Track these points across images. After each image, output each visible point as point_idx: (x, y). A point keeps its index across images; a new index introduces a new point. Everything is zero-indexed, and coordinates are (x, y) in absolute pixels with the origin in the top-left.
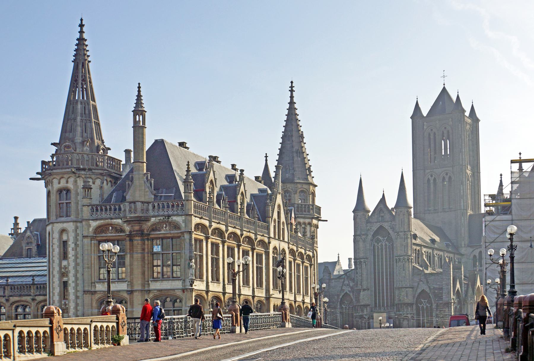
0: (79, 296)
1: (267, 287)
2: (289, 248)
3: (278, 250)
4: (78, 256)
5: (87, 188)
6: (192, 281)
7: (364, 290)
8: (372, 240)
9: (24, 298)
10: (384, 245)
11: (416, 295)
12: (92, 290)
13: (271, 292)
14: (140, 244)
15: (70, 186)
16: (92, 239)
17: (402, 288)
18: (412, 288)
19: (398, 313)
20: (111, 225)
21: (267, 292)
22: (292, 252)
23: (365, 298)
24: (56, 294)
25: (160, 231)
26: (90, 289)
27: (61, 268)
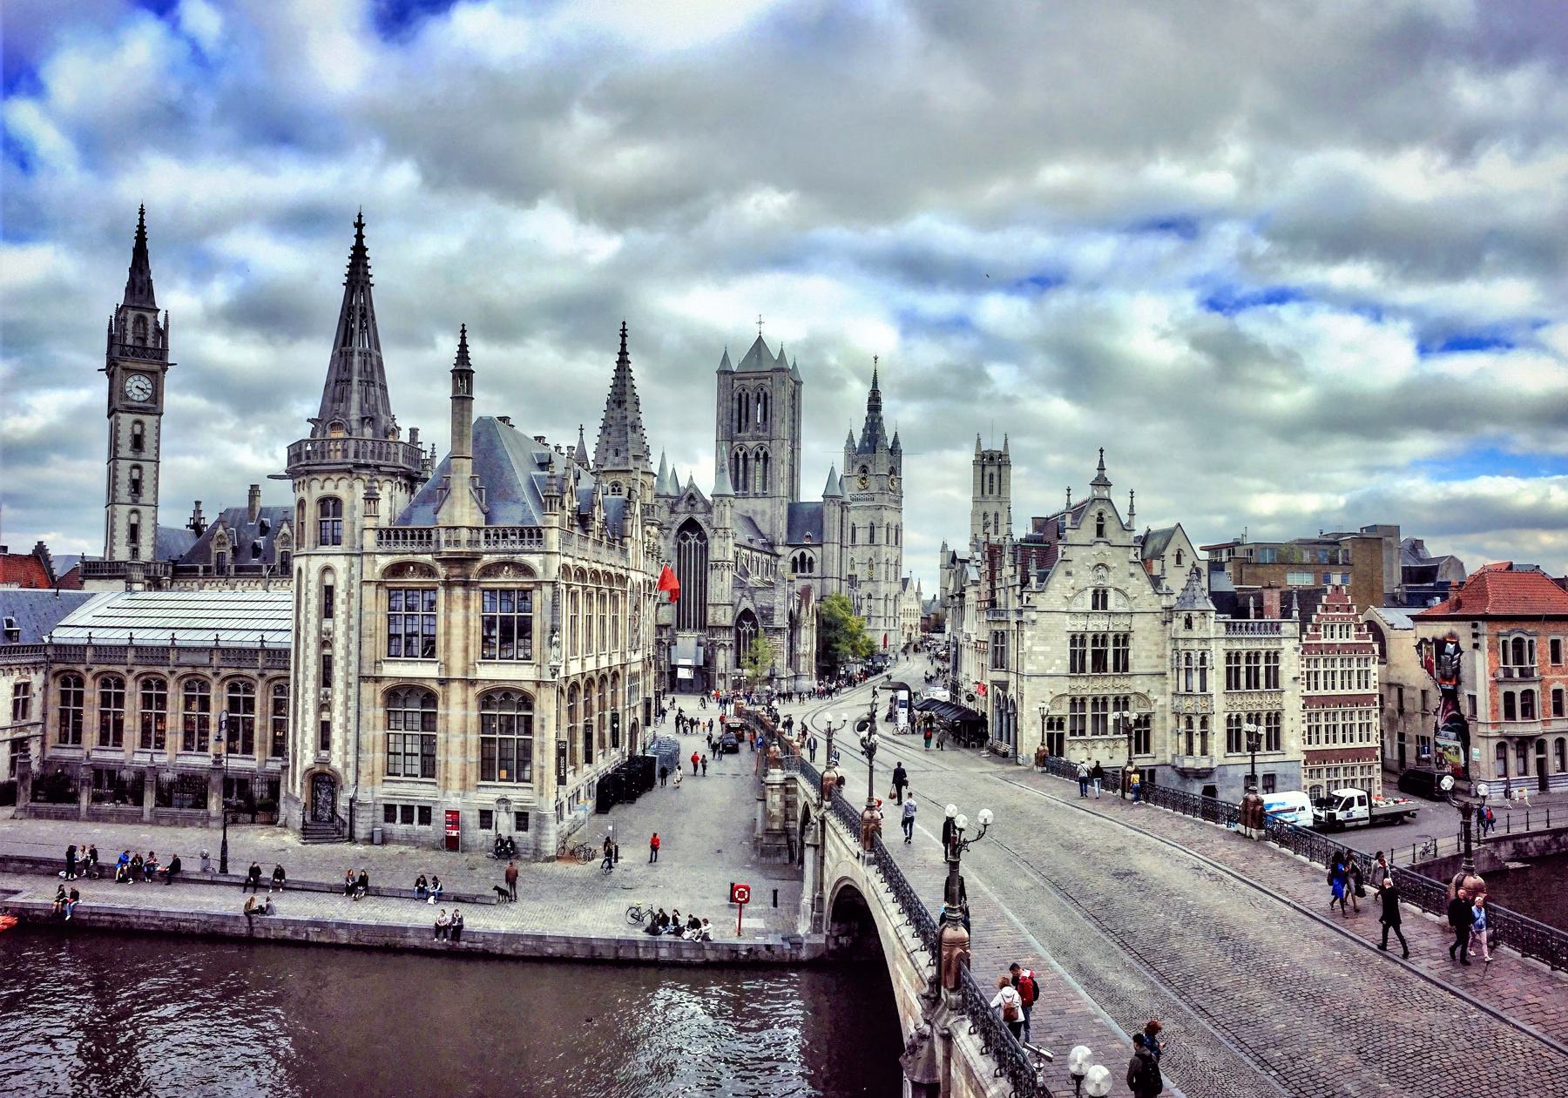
5: (371, 498)
15: (342, 492)
20: (412, 563)
24: (311, 677)
25: (496, 576)
27: (320, 632)
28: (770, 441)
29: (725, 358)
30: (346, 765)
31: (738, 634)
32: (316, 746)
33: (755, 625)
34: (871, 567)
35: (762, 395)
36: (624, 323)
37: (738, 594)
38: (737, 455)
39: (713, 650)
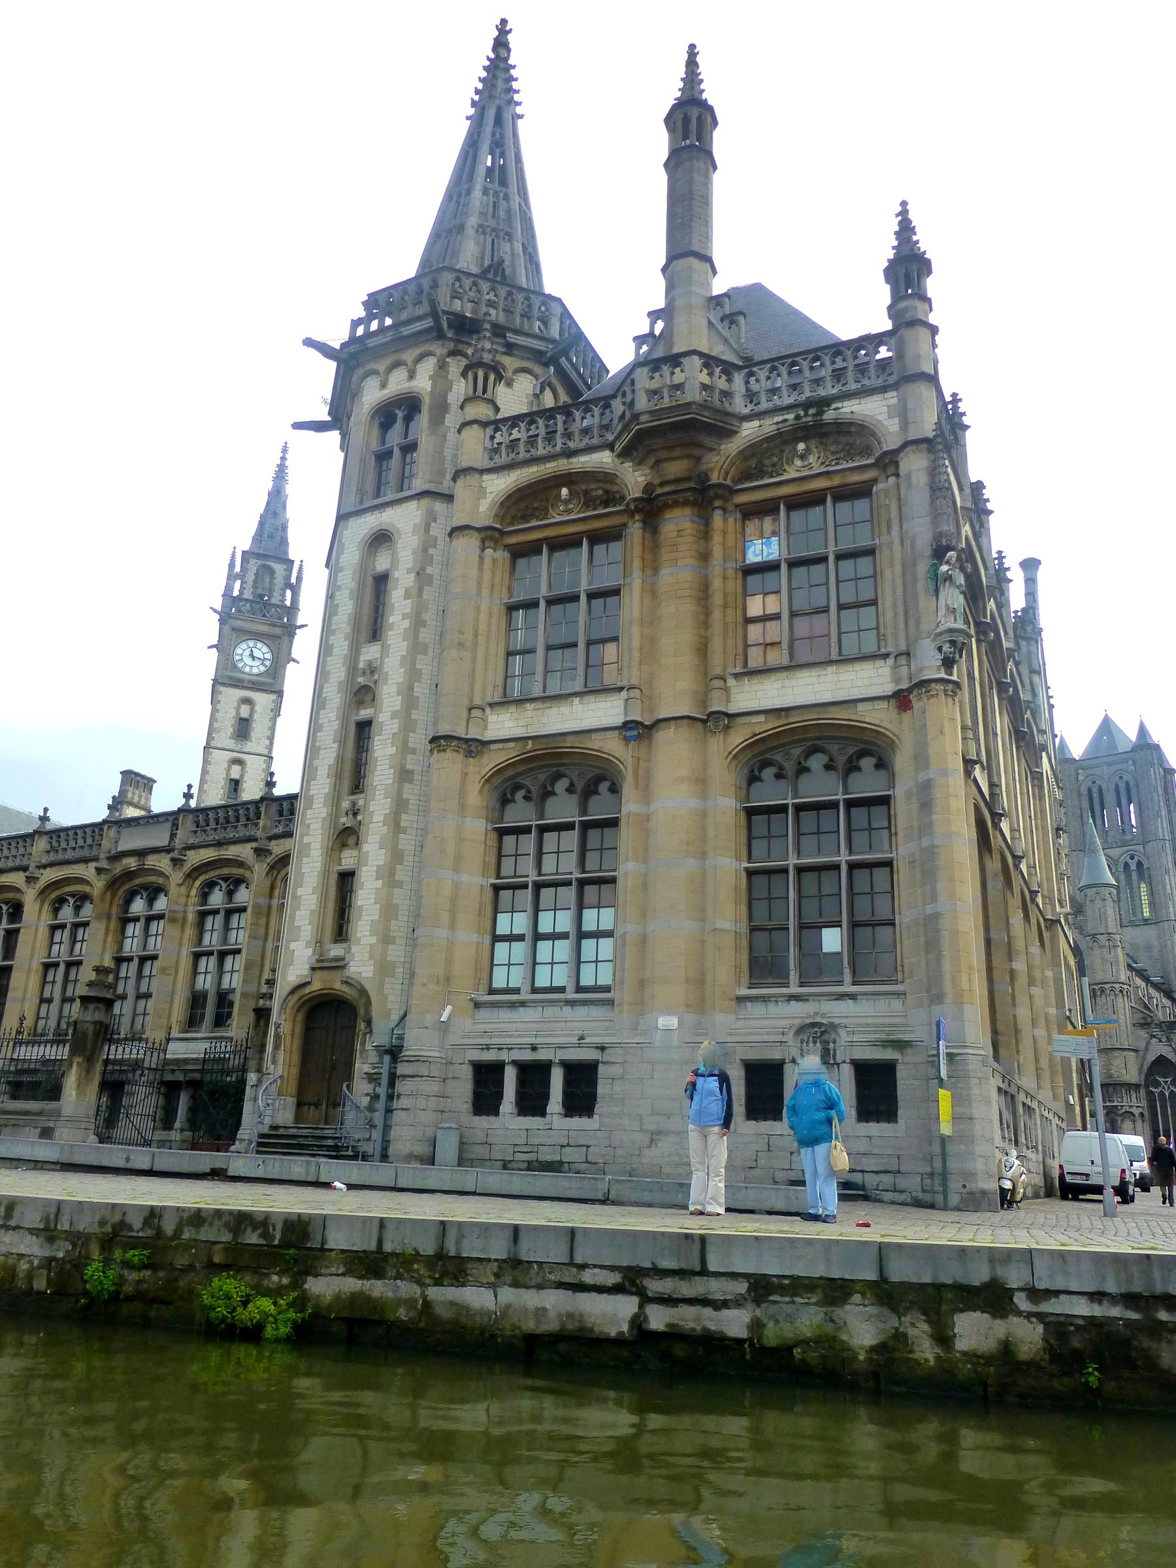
0: (411, 772)
4: (425, 616)
6: (953, 643)
9: (232, 851)
11: (1145, 1067)
12: (468, 737)
14: (688, 532)
16: (487, 544)
20: (568, 479)
26: (460, 732)
27: (352, 670)
30: (384, 969)
31: (1150, 1094)
32: (320, 929)
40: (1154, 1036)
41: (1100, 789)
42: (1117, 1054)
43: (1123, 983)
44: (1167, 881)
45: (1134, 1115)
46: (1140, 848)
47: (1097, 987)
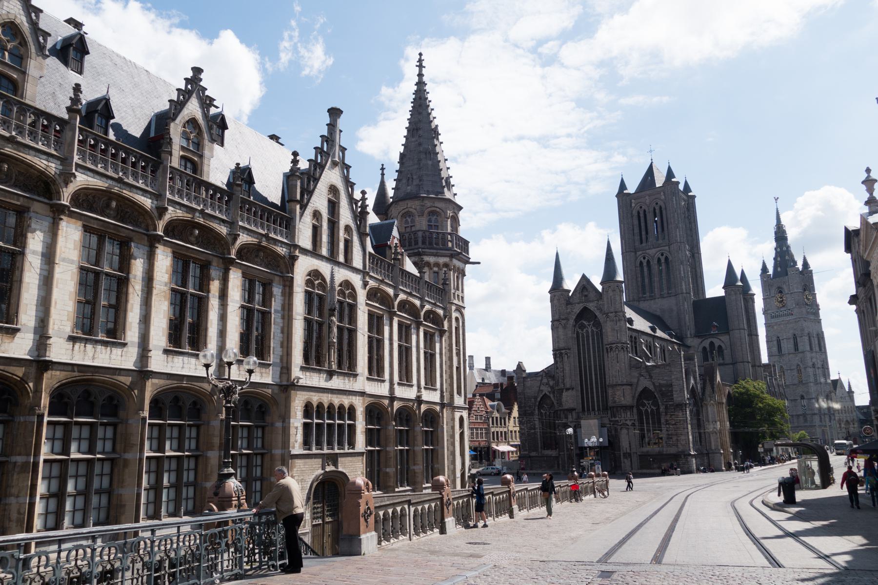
1: (285, 361)
2: (365, 284)
3: (328, 280)
7: (567, 389)
8: (575, 326)
10: (590, 330)
11: (637, 395)
13: (296, 372)
17: (616, 385)
18: (631, 385)
19: (613, 419)
21: (285, 371)
22: (373, 294)
23: (570, 399)
28: (669, 246)
29: (623, 186)
31: (640, 413)
33: (656, 403)
34: (799, 371)
35: (657, 208)
36: (420, 54)
37: (635, 374)
38: (641, 263)
39: (616, 430)
40: (643, 376)
41: (645, 211)
42: (618, 388)
43: (624, 343)
44: (682, 269)
45: (628, 425)
46: (667, 248)
47: (608, 346)
